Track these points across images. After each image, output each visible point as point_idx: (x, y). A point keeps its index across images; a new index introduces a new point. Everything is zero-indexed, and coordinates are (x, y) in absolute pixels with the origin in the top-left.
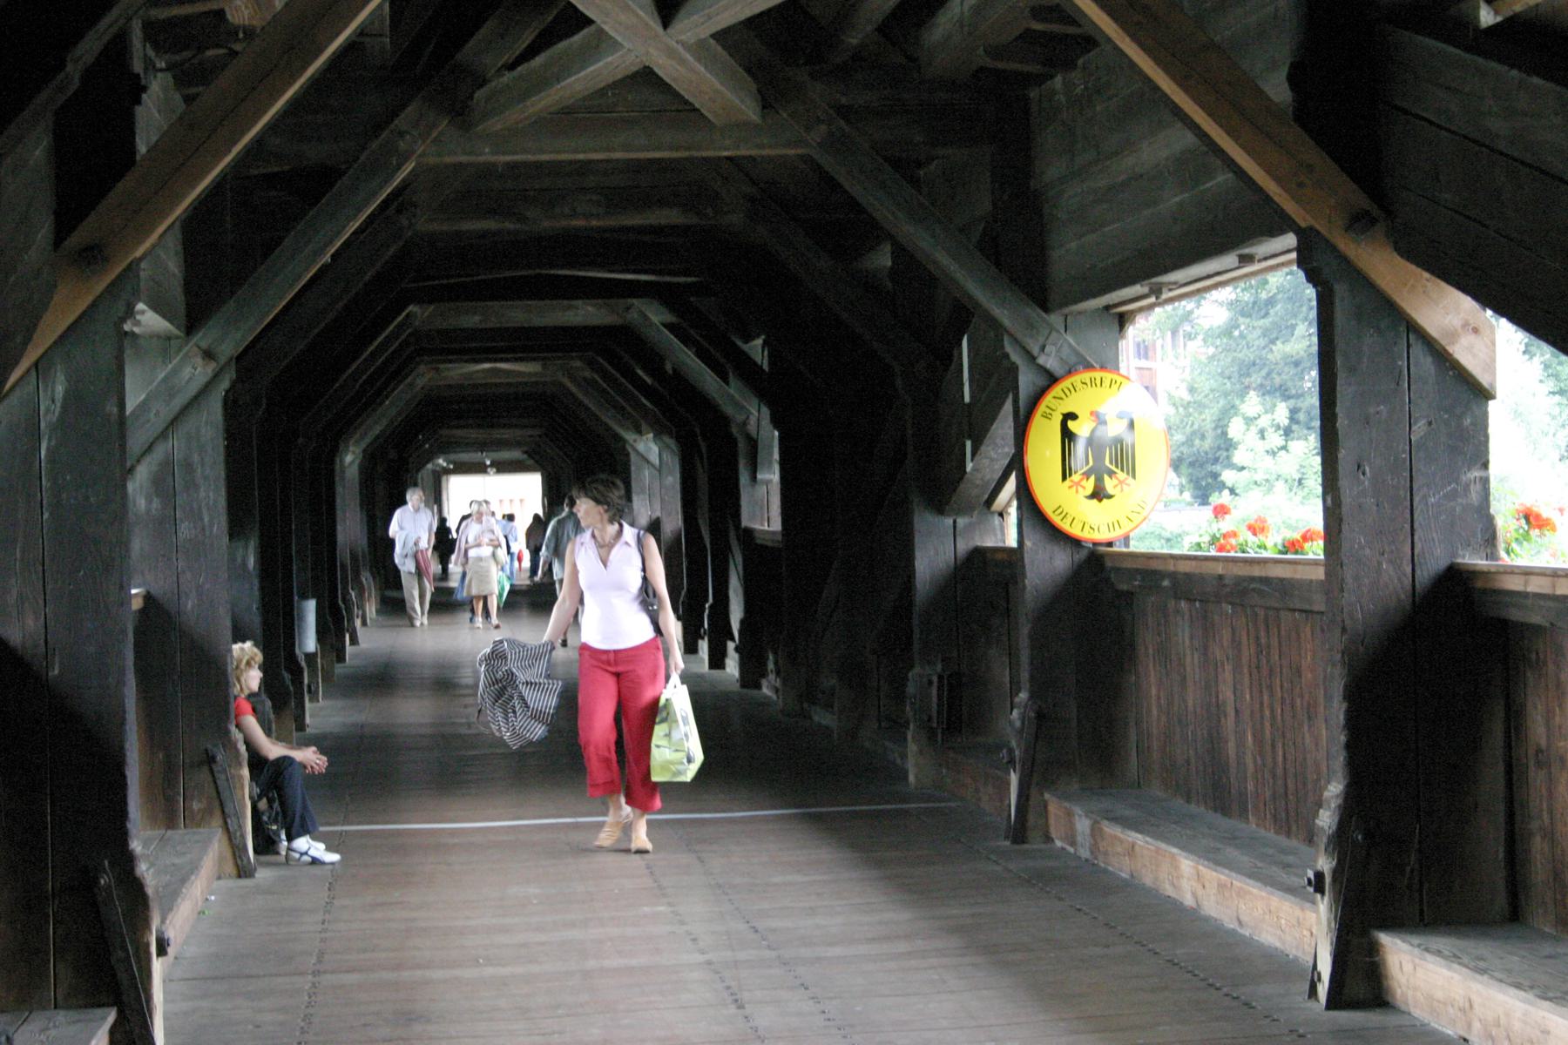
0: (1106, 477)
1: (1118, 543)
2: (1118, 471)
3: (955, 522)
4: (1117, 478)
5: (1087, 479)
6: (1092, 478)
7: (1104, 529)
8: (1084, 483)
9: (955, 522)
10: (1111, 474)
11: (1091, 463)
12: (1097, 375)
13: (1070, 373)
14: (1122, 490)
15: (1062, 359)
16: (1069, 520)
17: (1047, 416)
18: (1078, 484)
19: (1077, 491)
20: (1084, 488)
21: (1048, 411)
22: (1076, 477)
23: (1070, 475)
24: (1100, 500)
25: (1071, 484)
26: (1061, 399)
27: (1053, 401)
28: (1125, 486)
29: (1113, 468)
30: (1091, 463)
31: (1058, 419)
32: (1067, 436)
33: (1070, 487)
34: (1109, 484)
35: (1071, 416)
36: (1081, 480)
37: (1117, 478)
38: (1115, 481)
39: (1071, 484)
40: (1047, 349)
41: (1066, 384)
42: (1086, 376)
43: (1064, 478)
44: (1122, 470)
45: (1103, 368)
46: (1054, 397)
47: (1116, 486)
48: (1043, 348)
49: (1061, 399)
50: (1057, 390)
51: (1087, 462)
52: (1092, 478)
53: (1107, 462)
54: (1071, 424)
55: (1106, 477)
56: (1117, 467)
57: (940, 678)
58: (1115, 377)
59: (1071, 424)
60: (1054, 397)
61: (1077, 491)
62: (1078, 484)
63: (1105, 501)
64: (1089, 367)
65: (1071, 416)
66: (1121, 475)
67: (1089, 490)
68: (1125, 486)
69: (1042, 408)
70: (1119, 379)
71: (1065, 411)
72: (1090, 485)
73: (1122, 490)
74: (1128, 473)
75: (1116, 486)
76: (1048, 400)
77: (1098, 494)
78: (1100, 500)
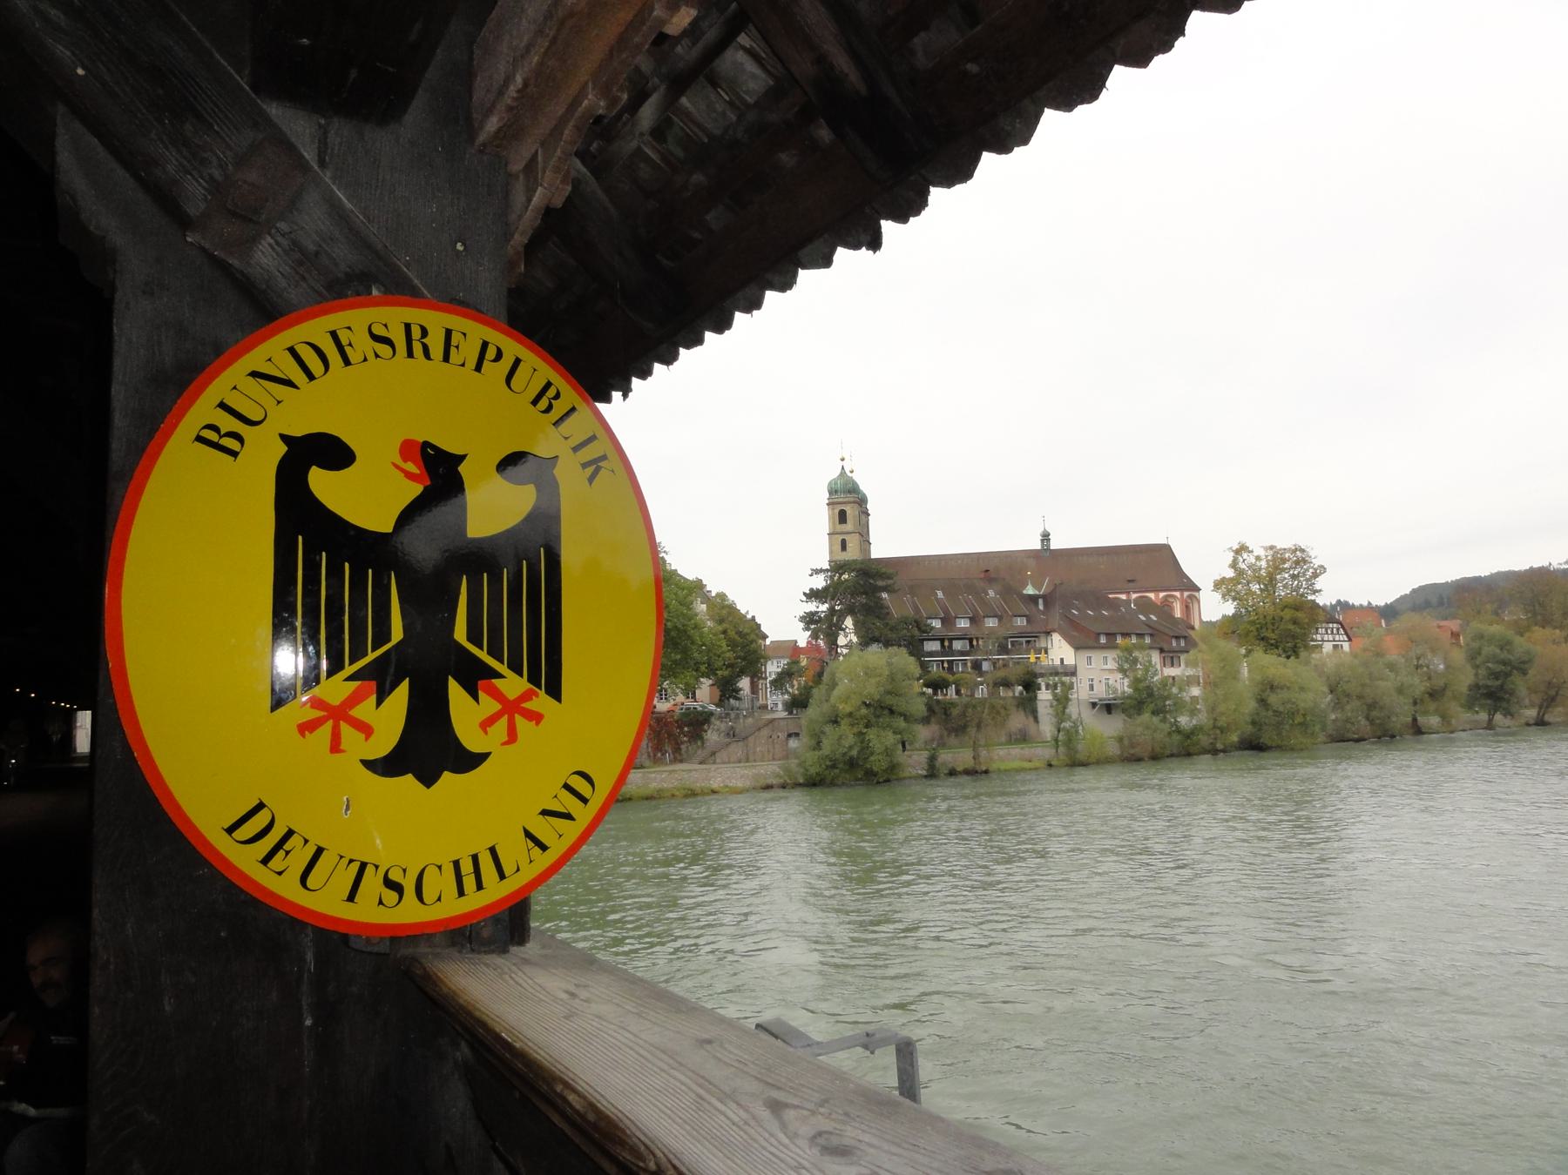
0: (455, 690)
2: (502, 668)
4: (497, 695)
7: (440, 883)
8: (365, 710)
10: (475, 677)
11: (397, 633)
12: (436, 321)
14: (512, 736)
16: (299, 857)
19: (335, 747)
20: (366, 729)
21: (228, 423)
24: (428, 779)
26: (289, 383)
28: (520, 721)
29: (483, 655)
30: (397, 633)
33: (306, 728)
35: (334, 453)
36: (355, 699)
37: (497, 695)
38: (489, 705)
42: (393, 318)
44: (516, 668)
46: (254, 374)
47: (486, 724)
49: (289, 383)
50: (271, 352)
51: (382, 635)
53: (460, 633)
54: (322, 483)
55: (455, 690)
56: (495, 652)
59: (322, 483)
60: (255, 374)
61: (335, 747)
66: (513, 685)
67: (386, 739)
68: (520, 721)
69: (202, 411)
71: (298, 432)
73: (512, 736)
74: (534, 679)
75: (486, 724)
78: (428, 779)
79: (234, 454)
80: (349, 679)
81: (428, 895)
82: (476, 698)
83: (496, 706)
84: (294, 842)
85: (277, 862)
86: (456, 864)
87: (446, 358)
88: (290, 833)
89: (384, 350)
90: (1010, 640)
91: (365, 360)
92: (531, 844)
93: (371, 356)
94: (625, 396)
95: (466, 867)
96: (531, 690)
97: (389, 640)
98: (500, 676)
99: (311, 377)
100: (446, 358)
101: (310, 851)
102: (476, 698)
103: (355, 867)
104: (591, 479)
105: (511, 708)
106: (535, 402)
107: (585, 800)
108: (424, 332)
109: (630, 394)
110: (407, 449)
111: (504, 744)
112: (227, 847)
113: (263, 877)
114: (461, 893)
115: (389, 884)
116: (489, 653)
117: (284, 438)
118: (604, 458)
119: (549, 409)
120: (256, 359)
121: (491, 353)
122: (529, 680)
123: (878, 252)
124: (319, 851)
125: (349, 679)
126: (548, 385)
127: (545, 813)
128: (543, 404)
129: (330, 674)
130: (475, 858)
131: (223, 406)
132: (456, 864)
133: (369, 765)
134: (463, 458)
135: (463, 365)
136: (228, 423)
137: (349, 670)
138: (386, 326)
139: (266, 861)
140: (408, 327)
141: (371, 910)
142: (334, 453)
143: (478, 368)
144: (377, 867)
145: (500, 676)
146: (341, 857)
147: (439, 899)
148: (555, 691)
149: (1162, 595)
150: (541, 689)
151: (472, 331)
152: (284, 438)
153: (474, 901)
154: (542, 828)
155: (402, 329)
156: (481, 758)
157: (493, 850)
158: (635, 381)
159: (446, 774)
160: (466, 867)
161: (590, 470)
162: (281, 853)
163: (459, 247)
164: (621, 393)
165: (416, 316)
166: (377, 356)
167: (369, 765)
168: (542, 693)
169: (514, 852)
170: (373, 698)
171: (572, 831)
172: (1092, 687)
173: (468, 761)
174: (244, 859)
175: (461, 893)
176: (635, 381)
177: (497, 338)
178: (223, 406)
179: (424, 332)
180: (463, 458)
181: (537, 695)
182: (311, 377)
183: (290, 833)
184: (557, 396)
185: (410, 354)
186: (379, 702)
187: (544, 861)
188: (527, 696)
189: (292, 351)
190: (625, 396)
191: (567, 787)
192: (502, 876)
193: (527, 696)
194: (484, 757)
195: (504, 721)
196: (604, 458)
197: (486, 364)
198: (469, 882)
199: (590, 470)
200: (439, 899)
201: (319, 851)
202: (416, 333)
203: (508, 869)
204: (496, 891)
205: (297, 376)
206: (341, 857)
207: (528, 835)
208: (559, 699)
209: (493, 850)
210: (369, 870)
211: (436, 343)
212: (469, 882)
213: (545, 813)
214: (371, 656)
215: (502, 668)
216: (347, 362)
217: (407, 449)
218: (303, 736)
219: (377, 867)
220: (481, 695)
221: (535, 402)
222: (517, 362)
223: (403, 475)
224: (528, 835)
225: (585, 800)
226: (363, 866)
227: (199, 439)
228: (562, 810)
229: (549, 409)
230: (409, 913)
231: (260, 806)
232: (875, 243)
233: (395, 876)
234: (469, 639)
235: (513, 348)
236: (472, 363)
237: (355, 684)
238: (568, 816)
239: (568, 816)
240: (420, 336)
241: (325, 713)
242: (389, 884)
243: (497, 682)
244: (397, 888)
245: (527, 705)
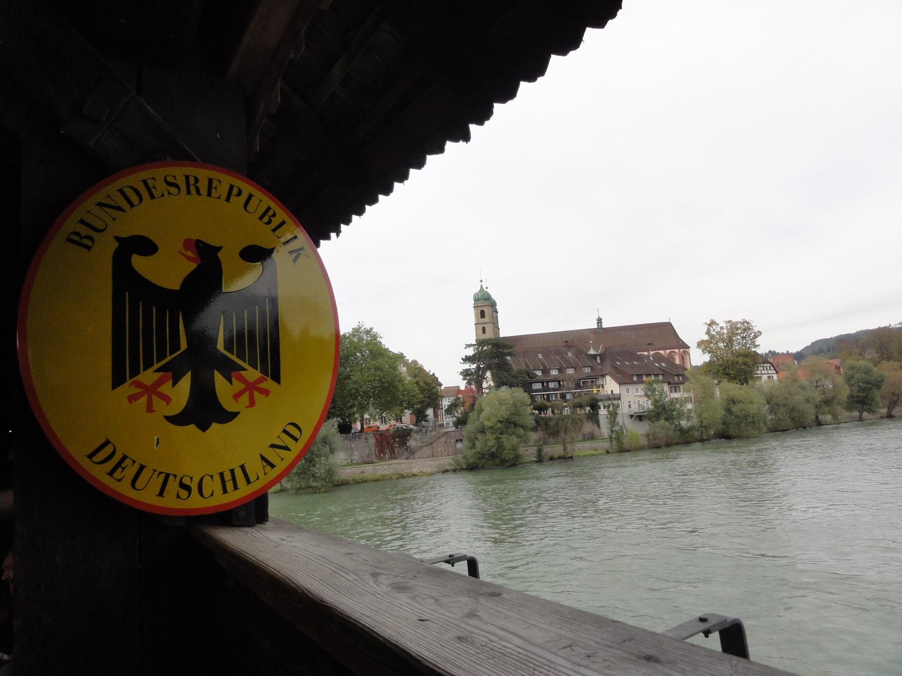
1: (242, 513)
2: (246, 365)
4: (243, 380)
6: (186, 382)
7: (212, 486)
8: (166, 388)
10: (229, 369)
12: (203, 174)
14: (252, 403)
18: (151, 391)
19: (150, 409)
21: (85, 231)
22: (148, 376)
23: (135, 372)
24: (204, 427)
25: (135, 390)
26: (119, 209)
27: (97, 211)
29: (234, 358)
31: (106, 248)
33: (132, 398)
34: (224, 389)
37: (243, 380)
38: (238, 386)
39: (135, 390)
42: (179, 173)
43: (118, 380)
46: (100, 204)
47: (237, 396)
49: (119, 209)
50: (109, 191)
51: (175, 346)
54: (139, 263)
56: (241, 356)
59: (139, 263)
60: (100, 204)
61: (150, 409)
62: (151, 391)
63: (215, 426)
66: (252, 374)
69: (71, 224)
71: (124, 235)
73: (252, 403)
74: (264, 371)
75: (237, 396)
78: (204, 427)
79: (89, 248)
80: (157, 371)
81: (206, 492)
82: (231, 382)
83: (242, 386)
84: (128, 462)
85: (117, 475)
86: (222, 475)
87: (209, 194)
88: (125, 458)
89: (174, 190)
90: (581, 381)
91: (163, 195)
92: (265, 464)
93: (166, 193)
94: (338, 235)
95: (228, 476)
96: (262, 377)
97: (179, 349)
98: (244, 369)
99: (132, 205)
100: (209, 194)
101: (136, 467)
102: (231, 382)
103: (162, 476)
104: (295, 260)
105: (251, 387)
106: (261, 218)
107: (296, 440)
108: (197, 180)
109: (341, 234)
110: (187, 244)
111: (247, 407)
114: (225, 491)
115: (183, 486)
116: (237, 357)
117: (117, 239)
118: (302, 249)
119: (269, 222)
120: (100, 196)
121: (235, 191)
122: (261, 372)
123: (469, 143)
124: (142, 467)
125: (157, 371)
126: (269, 209)
127: (272, 446)
128: (266, 219)
129: (144, 370)
130: (232, 471)
131: (82, 222)
132: (222, 475)
134: (220, 248)
135: (219, 198)
136: (85, 231)
137: (157, 366)
138: (174, 177)
139: (111, 474)
140: (187, 177)
141: (171, 502)
142: (147, 247)
143: (228, 199)
144: (175, 476)
145: (244, 369)
146: (155, 471)
147: (212, 495)
148: (277, 378)
149: (668, 351)
150: (268, 376)
151: (224, 180)
152: (117, 239)
153: (233, 496)
154: (271, 455)
155: (184, 179)
156: (234, 415)
157: (242, 467)
158: (343, 227)
159: (214, 424)
160: (228, 476)
161: (295, 255)
162: (120, 469)
163: (218, 136)
164: (335, 234)
165: (192, 171)
166: (169, 193)
167: (170, 419)
168: (269, 379)
169: (255, 467)
170: (170, 383)
171: (289, 457)
172: (630, 406)
173: (228, 417)
174: (99, 473)
175: (225, 491)
176: (343, 227)
177: (239, 183)
178: (82, 222)
179: (197, 180)
180: (220, 248)
181: (266, 380)
182: (132, 205)
183: (125, 458)
184: (274, 215)
185: (189, 192)
186: (174, 385)
189: (121, 191)
190: (338, 235)
191: (285, 431)
192: (249, 482)
193: (260, 380)
194: (238, 413)
195: (247, 394)
196: (302, 249)
197: (233, 198)
198: (229, 485)
199: (295, 255)
200: (212, 495)
201: (142, 467)
202: (192, 181)
203: (252, 478)
204: (245, 491)
206: (155, 471)
207: (263, 458)
208: (279, 383)
209: (242, 467)
210: (171, 478)
211: (203, 187)
212: (229, 485)
213: (272, 446)
214: (169, 358)
215: (246, 365)
216: (152, 197)
217: (187, 244)
218: (131, 403)
219: (175, 476)
220: (233, 380)
221: (261, 218)
222: (251, 196)
223: (184, 258)
224: (263, 458)
225: (296, 440)
226: (167, 476)
227: (69, 240)
228: (283, 444)
229: (269, 222)
230: (195, 503)
231: (107, 442)
232: (466, 137)
233: (186, 481)
234: (225, 349)
235: (247, 188)
236: (224, 196)
237: (159, 374)
238: (286, 448)
239: (286, 448)
240: (194, 182)
241: (143, 390)
242: (183, 486)
243: (243, 373)
244: (187, 488)
245: (261, 385)
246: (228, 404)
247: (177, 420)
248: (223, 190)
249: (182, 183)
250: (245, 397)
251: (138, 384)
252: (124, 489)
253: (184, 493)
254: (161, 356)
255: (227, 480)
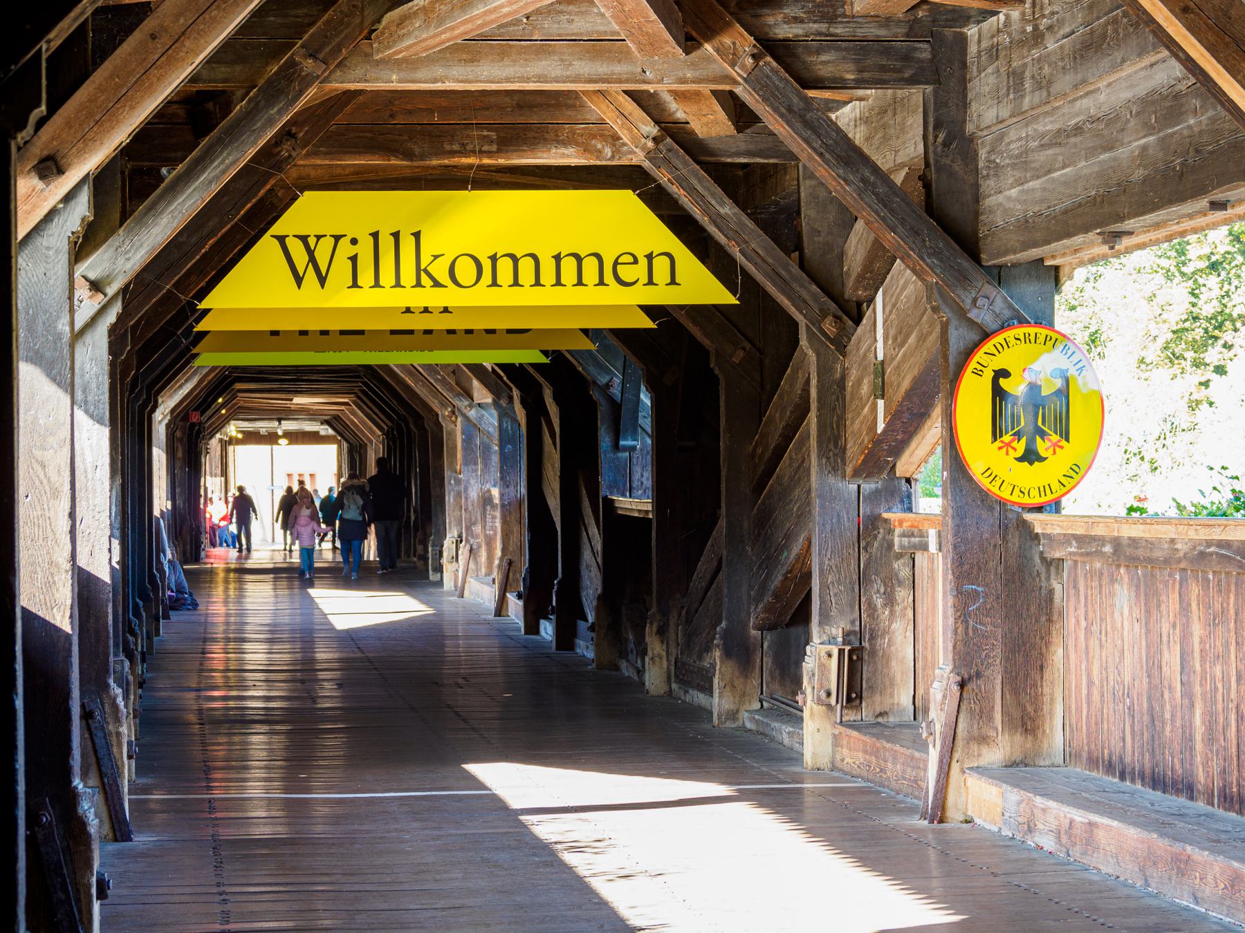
0: (1038, 439)
1: (1048, 508)
2: (1052, 433)
3: (859, 486)
4: (1050, 440)
5: (1019, 440)
8: (1014, 444)
9: (859, 486)
10: (1043, 434)
12: (1032, 330)
13: (1003, 328)
14: (1054, 452)
15: (994, 311)
17: (977, 373)
19: (1007, 453)
20: (1015, 449)
21: (980, 367)
22: (1007, 438)
24: (1031, 463)
25: (1001, 445)
31: (988, 375)
32: (998, 394)
33: (1000, 448)
34: (1042, 446)
36: (1013, 440)
37: (1050, 440)
38: (1048, 444)
39: (1001, 445)
40: (979, 302)
41: (999, 339)
42: (1020, 332)
43: (995, 439)
45: (1038, 324)
47: (1047, 449)
48: (975, 301)
50: (989, 346)
51: (1019, 424)
52: (1024, 440)
54: (1003, 382)
57: (841, 652)
58: (1050, 333)
59: (1003, 382)
61: (1007, 453)
62: (1008, 445)
63: (1036, 463)
64: (1023, 322)
65: (1003, 373)
66: (1055, 438)
67: (1020, 453)
69: (973, 365)
70: (1054, 336)
71: (996, 369)
72: (1021, 447)
73: (1054, 452)
74: (1061, 435)
75: (1047, 449)
76: (979, 356)
77: (1030, 456)
81: (1032, 496)
85: (993, 483)
89: (1018, 342)
95: (1042, 489)
102: (1043, 440)
105: (1055, 445)
112: (980, 477)
113: (990, 487)
120: (985, 349)
133: (1016, 459)
148: (1067, 440)
153: (1043, 499)
154: (1063, 480)
160: (1042, 489)
167: (1016, 459)
169: (1055, 486)
171: (1073, 482)
174: (985, 482)
187: (1064, 490)
188: (1060, 441)
193: (1060, 441)
198: (1043, 494)
204: (1050, 497)
205: (996, 352)
212: (1043, 494)
230: (1026, 500)
246: (1043, 453)
247: (1020, 459)
248: (1041, 339)
249: (1022, 337)
250: (1051, 451)
251: (1002, 442)
252: (995, 490)
253: (1022, 495)
254: (1013, 429)
255: (1042, 491)
